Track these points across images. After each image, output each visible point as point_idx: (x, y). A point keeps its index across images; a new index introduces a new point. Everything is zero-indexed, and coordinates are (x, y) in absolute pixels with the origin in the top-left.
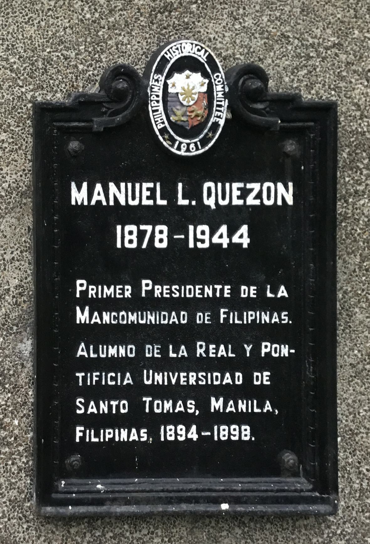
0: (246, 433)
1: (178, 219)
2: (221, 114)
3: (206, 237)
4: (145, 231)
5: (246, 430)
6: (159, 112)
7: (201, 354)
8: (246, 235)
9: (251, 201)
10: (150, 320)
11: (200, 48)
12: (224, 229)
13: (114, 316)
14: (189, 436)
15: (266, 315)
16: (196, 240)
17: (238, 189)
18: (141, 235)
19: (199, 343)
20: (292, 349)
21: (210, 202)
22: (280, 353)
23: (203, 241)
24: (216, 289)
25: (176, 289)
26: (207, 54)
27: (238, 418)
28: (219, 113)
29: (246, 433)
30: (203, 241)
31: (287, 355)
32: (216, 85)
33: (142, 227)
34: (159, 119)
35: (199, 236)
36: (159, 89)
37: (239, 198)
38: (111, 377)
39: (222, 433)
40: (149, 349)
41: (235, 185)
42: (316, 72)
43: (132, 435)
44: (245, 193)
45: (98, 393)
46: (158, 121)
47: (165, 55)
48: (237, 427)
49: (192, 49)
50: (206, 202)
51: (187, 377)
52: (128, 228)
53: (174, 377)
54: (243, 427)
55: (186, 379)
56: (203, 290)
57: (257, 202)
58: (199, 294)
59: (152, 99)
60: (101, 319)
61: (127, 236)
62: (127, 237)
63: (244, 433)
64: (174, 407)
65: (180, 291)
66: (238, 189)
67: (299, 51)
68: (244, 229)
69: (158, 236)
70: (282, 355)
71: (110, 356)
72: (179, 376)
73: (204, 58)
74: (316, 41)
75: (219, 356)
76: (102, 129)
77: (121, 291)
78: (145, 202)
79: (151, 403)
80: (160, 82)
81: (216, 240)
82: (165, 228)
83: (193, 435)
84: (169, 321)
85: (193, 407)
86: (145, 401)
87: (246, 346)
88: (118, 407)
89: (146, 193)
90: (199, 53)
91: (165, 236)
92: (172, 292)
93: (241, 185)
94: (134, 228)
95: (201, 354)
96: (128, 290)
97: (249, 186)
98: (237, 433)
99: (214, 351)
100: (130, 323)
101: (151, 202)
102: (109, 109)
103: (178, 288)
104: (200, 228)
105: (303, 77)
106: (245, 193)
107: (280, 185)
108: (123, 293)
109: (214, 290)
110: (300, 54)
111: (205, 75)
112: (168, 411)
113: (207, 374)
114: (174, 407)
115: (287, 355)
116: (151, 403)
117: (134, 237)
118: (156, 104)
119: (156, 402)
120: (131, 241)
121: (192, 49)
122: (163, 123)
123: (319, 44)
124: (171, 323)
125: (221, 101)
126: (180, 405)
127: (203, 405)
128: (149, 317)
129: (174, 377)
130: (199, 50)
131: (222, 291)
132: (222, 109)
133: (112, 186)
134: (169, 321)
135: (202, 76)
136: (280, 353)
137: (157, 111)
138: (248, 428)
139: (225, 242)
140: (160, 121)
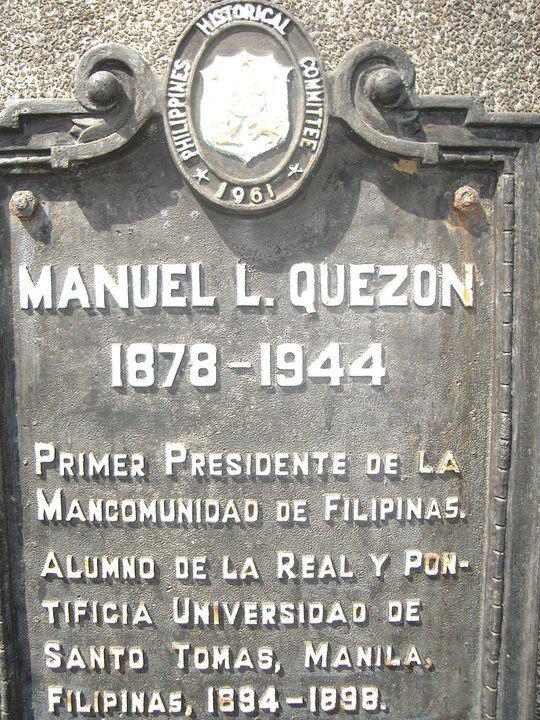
0: (370, 697)
2: (317, 131)
3: (297, 365)
4: (170, 356)
5: (370, 694)
6: (185, 129)
7: (284, 573)
8: (377, 361)
9: (387, 296)
10: (184, 516)
11: (271, 12)
12: (332, 350)
13: (111, 508)
14: (263, 704)
16: (274, 370)
17: (363, 275)
18: (161, 361)
19: (281, 555)
20: (464, 559)
21: (306, 300)
22: (440, 568)
23: (290, 373)
24: (317, 461)
25: (234, 461)
26: (287, 22)
27: (358, 676)
28: (312, 131)
29: (370, 697)
30: (290, 373)
31: (453, 571)
32: (305, 78)
33: (163, 348)
34: (183, 142)
35: (281, 364)
36: (185, 87)
37: (364, 292)
38: (109, 610)
39: (324, 700)
40: (182, 565)
41: (356, 270)
42: (523, 73)
43: (152, 702)
44: (375, 281)
46: (181, 146)
47: (198, 25)
48: (353, 689)
49: (254, 15)
50: (296, 300)
51: (259, 611)
53: (231, 611)
54: (365, 690)
55: (255, 615)
56: (288, 461)
57: (402, 300)
58: (282, 469)
59: (170, 104)
60: (85, 511)
61: (131, 363)
62: (133, 367)
63: (365, 698)
64: (232, 658)
65: (242, 464)
66: (363, 275)
67: (490, 33)
68: (374, 350)
69: (195, 364)
70: (444, 571)
71: (104, 576)
72: (241, 611)
73: (281, 29)
74: (524, 18)
75: (321, 575)
76: (66, 164)
77: (122, 465)
78: (169, 301)
79: (188, 653)
80: (187, 74)
81: (315, 370)
82: (210, 349)
83: (269, 702)
84: (221, 517)
85: (270, 660)
86: (177, 651)
87: (374, 559)
88: (123, 659)
89: (169, 285)
90: (269, 21)
91: (210, 364)
92: (224, 466)
93: (369, 268)
94: (146, 349)
95: (284, 573)
96: (137, 462)
97: (384, 270)
98: (353, 698)
99: (312, 568)
100: (142, 519)
101: (180, 302)
102: (83, 127)
103: (239, 459)
104: (283, 349)
105: (500, 81)
106: (375, 281)
108: (127, 467)
109: (312, 462)
110: (492, 39)
111: (284, 57)
112: (221, 667)
113: (296, 606)
114: (232, 658)
115: (453, 571)
116: (188, 653)
117: (147, 366)
118: (179, 114)
119: (198, 651)
120: (140, 374)
121: (254, 15)
122: (193, 149)
123: (530, 22)
124: (225, 520)
125: (316, 108)
126: (245, 656)
127: (287, 652)
128: (182, 509)
129: (231, 611)
130: (268, 16)
131: (328, 462)
132: (318, 122)
134: (221, 517)
135: (278, 58)
136: (440, 568)
137: (181, 126)
138: (374, 691)
139: (335, 374)
140: (186, 146)
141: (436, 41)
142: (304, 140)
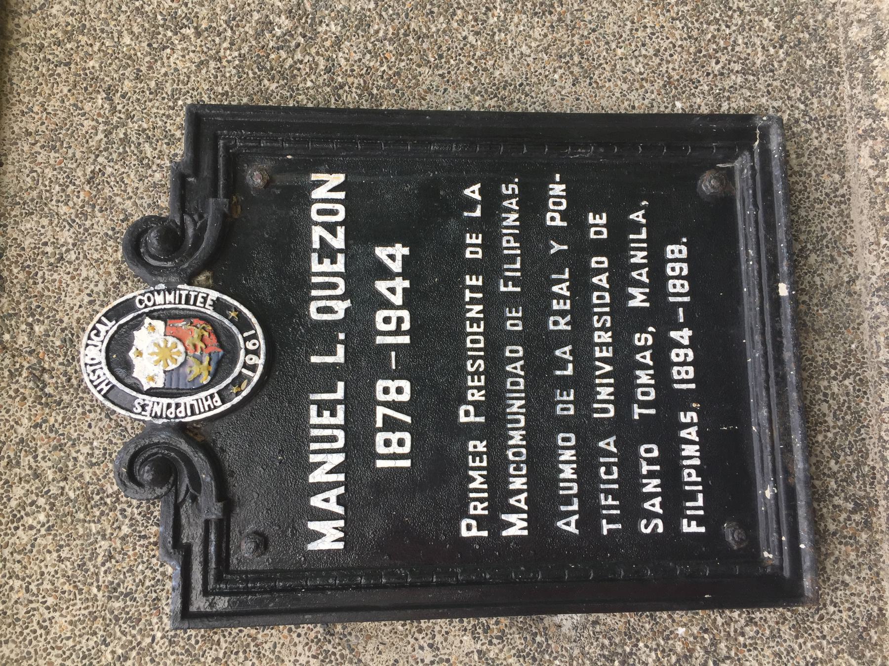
0: (676, 251)
1: (367, 362)
2: (200, 295)
3: (394, 314)
4: (385, 417)
6: (195, 403)
7: (566, 324)
8: (390, 250)
9: (338, 242)
10: (519, 407)
11: (95, 332)
12: (382, 286)
13: (515, 469)
14: (686, 342)
15: (508, 218)
16: (398, 332)
17: (320, 262)
18: (391, 425)
19: (552, 327)
21: (341, 307)
22: (561, 197)
23: (400, 320)
26: (104, 319)
27: (657, 263)
28: (200, 299)
29: (676, 251)
30: (400, 320)
31: (563, 187)
32: (154, 305)
33: (379, 423)
34: (206, 404)
36: (158, 403)
38: (606, 473)
39: (679, 289)
40: (562, 409)
41: (316, 267)
43: (689, 437)
45: (630, 494)
46: (209, 406)
47: (103, 393)
48: (670, 265)
49: (96, 346)
50: (341, 315)
51: (601, 345)
52: (381, 449)
53: (602, 368)
55: (604, 348)
56: (473, 320)
57: (341, 231)
59: (173, 416)
61: (393, 449)
62: (395, 449)
63: (677, 255)
64: (645, 367)
66: (320, 262)
67: (115, 156)
68: (381, 253)
69: (393, 396)
70: (564, 194)
71: (575, 477)
72: (601, 360)
73: (110, 324)
74: (101, 127)
75: (568, 294)
78: (340, 419)
79: (644, 405)
80: (146, 402)
81: (398, 300)
82: (381, 384)
83: (683, 335)
85: (644, 336)
86: (640, 414)
87: (552, 251)
88: (650, 461)
89: (326, 419)
90: (103, 334)
91: (392, 385)
92: (477, 372)
93: (315, 257)
94: (380, 438)
95: (566, 324)
96: (475, 447)
97: (316, 245)
98: (677, 266)
99: (562, 301)
100: (524, 443)
101: (341, 409)
102: (187, 491)
103: (471, 361)
104: (381, 326)
105: (156, 149)
106: (328, 253)
107: (317, 194)
108: (480, 454)
109: (473, 301)
110: (120, 154)
111: (136, 324)
112: (652, 377)
113: (596, 314)
114: (645, 367)
115: (563, 187)
117: (395, 437)
118: (182, 408)
119: (641, 398)
121: (96, 346)
122: (212, 396)
123: (106, 123)
124: (522, 373)
125: (180, 295)
126: (642, 357)
129: (602, 368)
130: (97, 335)
131: (473, 289)
132: (193, 294)
133: (316, 477)
134: (520, 376)
136: (561, 197)
137: (192, 406)
138: (669, 248)
139: (401, 284)
140: (210, 402)
141: (121, 200)
142: (207, 306)
